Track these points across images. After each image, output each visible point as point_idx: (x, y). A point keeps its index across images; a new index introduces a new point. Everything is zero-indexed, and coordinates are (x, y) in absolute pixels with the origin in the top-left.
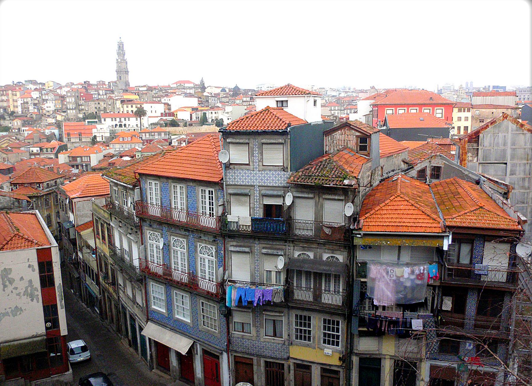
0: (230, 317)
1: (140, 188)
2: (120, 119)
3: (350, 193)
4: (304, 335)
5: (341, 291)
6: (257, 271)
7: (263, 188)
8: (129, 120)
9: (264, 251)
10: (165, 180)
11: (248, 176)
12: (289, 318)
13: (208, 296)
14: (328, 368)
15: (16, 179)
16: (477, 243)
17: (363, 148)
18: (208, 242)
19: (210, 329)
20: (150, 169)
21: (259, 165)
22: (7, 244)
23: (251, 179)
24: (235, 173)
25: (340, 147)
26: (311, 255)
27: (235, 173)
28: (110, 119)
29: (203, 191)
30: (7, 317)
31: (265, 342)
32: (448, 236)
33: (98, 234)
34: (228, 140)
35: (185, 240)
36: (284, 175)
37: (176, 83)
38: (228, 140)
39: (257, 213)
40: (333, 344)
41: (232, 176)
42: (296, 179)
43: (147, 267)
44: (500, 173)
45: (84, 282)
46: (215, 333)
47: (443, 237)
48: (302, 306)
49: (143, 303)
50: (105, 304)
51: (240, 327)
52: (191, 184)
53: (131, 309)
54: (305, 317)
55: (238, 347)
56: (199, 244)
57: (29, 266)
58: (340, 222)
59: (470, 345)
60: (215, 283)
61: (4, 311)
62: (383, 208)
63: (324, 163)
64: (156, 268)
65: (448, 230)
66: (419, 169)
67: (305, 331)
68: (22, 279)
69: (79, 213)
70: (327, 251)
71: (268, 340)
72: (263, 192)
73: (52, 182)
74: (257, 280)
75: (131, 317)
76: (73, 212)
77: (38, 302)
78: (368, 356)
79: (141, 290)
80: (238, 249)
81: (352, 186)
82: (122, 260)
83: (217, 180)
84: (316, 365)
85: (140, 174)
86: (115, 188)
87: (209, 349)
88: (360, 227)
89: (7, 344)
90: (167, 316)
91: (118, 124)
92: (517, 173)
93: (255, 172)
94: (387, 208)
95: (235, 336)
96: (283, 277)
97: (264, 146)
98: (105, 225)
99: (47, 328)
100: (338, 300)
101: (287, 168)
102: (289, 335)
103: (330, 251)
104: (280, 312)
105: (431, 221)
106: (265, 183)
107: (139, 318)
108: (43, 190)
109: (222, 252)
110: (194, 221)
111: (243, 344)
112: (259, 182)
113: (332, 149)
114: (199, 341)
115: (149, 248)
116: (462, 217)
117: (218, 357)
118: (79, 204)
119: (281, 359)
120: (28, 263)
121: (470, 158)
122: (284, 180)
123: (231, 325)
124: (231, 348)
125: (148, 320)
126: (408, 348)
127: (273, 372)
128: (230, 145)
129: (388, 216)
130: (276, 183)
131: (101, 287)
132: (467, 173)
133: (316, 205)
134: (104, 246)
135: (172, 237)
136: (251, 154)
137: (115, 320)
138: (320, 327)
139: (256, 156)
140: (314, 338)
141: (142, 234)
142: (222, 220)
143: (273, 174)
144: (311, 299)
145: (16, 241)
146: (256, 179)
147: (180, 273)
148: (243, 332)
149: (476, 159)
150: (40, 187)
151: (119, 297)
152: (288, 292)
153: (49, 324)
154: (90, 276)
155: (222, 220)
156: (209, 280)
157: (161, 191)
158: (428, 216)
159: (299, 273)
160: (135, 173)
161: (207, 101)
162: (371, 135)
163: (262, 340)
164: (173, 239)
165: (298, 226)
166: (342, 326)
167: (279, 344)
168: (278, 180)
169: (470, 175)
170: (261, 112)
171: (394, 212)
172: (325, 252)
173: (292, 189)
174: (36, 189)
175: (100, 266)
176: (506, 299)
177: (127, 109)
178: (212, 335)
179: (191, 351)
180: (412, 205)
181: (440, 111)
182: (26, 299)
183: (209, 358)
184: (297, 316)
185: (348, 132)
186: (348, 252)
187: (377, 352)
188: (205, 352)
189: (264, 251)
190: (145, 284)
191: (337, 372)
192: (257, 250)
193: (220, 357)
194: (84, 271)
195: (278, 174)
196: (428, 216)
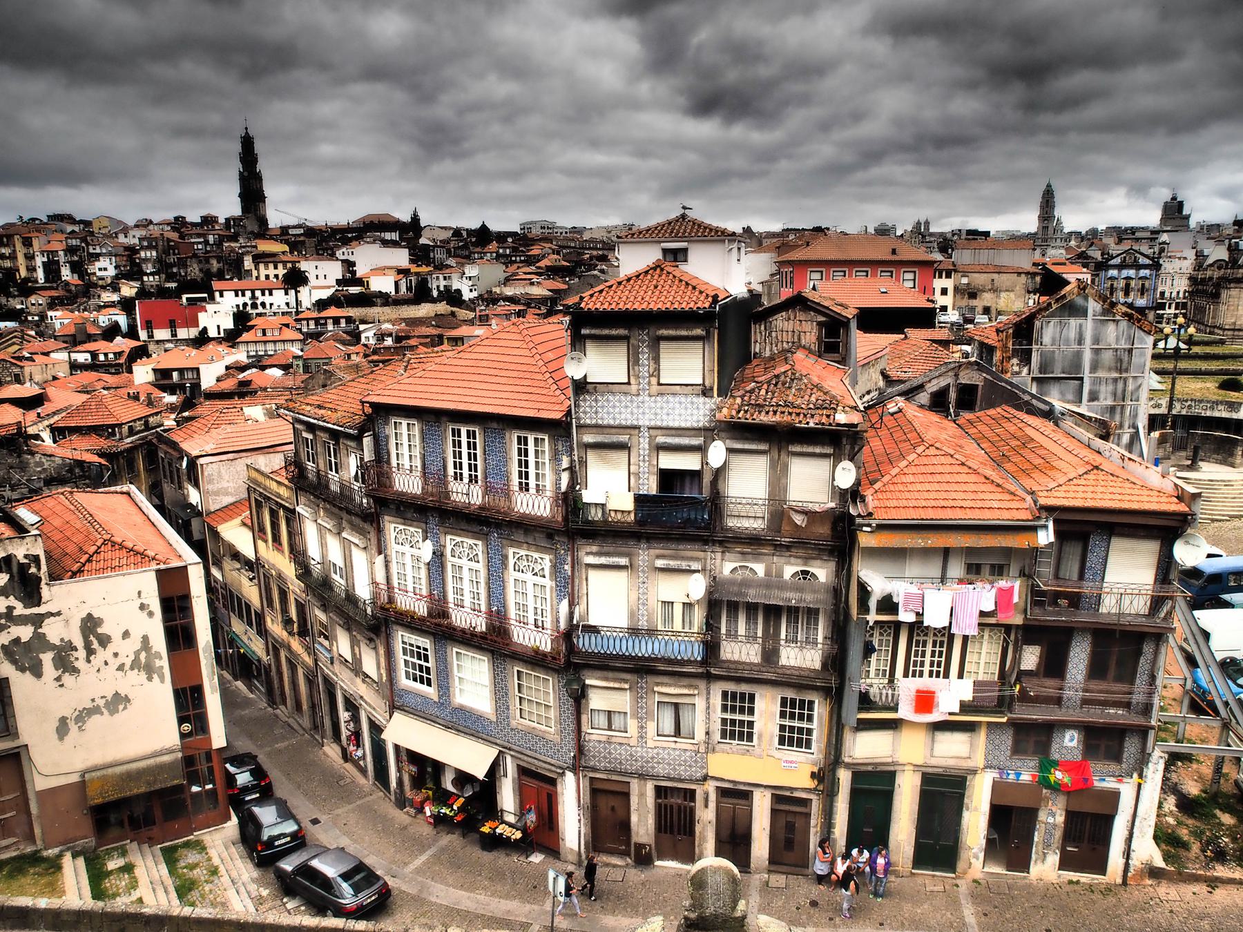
2: (253, 292)
4: (738, 731)
5: (820, 639)
6: (643, 604)
7: (659, 432)
8: (271, 294)
9: (660, 563)
10: (432, 417)
12: (708, 699)
13: (536, 660)
14: (788, 794)
15: (70, 415)
16: (1095, 542)
18: (533, 548)
19: (535, 725)
20: (396, 393)
22: (89, 561)
24: (596, 401)
26: (760, 569)
27: (596, 401)
29: (523, 441)
30: (96, 717)
32: (1046, 527)
33: (262, 530)
34: (583, 332)
35: (480, 543)
38: (583, 332)
40: (799, 745)
41: (591, 407)
42: (734, 413)
44: (1070, 397)
45: (226, 628)
47: (1034, 529)
48: (737, 673)
49: (380, 675)
50: (280, 673)
51: (602, 720)
52: (495, 425)
53: (346, 682)
54: (743, 695)
55: (599, 761)
56: (511, 551)
57: (142, 607)
58: (822, 500)
59: (1072, 740)
61: (89, 705)
62: (906, 470)
63: (782, 378)
64: (413, 602)
65: (1044, 515)
66: (935, 389)
68: (126, 634)
69: (210, 487)
70: (792, 560)
71: (665, 745)
72: (661, 439)
74: (643, 624)
76: (196, 485)
77: (162, 681)
78: (870, 768)
79: (375, 648)
80: (603, 560)
81: (856, 426)
82: (326, 583)
84: (762, 789)
85: (372, 405)
86: (305, 435)
87: (534, 765)
89: (99, 774)
91: (249, 303)
92: (1102, 396)
93: (640, 398)
94: (914, 469)
95: (593, 737)
96: (699, 616)
97: (663, 345)
98: (281, 512)
99: (183, 736)
100: (752, 653)
101: (712, 389)
102: (707, 733)
104: (690, 686)
105: (1007, 497)
107: (370, 705)
110: (502, 504)
111: (610, 753)
116: (1064, 488)
117: (553, 782)
118: (210, 468)
119: (691, 781)
120: (140, 601)
121: (1016, 369)
123: (584, 718)
124: (583, 762)
125: (393, 708)
126: (953, 750)
127: (671, 807)
129: (919, 487)
131: (270, 639)
132: (1027, 398)
133: (773, 466)
135: (449, 537)
136: (633, 361)
137: (305, 707)
140: (760, 736)
142: (570, 501)
145: (107, 553)
147: (468, 614)
148: (610, 728)
149: (1025, 370)
151: (316, 660)
152: (711, 648)
153: (187, 727)
154: (241, 617)
155: (570, 501)
156: (536, 626)
157: (423, 439)
158: (998, 485)
159: (733, 607)
160: (363, 403)
163: (650, 744)
164: (449, 541)
165: (731, 508)
166: (820, 710)
169: (1034, 402)
170: (646, 272)
171: (930, 478)
172: (789, 563)
173: (723, 434)
176: (1148, 649)
179: (494, 770)
180: (963, 464)
181: (910, 276)
182: (138, 677)
183: (533, 783)
184: (725, 694)
185: (801, 316)
186: (838, 563)
187: (890, 760)
188: (523, 771)
189: (660, 563)
191: (806, 803)
192: (643, 561)
193: (559, 780)
194: (224, 606)
196: (998, 485)
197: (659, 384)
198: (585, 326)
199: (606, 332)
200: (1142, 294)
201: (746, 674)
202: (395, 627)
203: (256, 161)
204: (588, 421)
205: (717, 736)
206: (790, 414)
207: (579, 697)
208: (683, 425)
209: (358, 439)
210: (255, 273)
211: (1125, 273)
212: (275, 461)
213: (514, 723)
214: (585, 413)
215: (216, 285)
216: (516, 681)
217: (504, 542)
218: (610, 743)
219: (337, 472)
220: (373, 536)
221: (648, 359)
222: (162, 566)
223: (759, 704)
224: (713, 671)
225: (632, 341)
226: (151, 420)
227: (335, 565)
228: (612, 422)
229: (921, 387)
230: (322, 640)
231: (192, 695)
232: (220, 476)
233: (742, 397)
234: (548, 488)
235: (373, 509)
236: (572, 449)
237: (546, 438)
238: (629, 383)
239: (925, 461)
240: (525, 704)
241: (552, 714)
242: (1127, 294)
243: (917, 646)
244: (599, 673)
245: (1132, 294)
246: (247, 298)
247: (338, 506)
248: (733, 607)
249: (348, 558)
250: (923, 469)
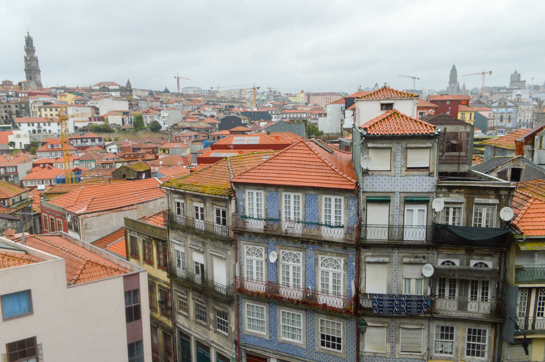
2: (39, 124)
8: (49, 125)
28: (26, 124)
37: (99, 85)
91: (37, 130)
161: (137, 105)
177: (46, 113)
200: (509, 121)
203: (34, 51)
210: (39, 113)
211: (500, 110)
215: (16, 120)
242: (501, 120)
245: (504, 121)
246: (35, 127)
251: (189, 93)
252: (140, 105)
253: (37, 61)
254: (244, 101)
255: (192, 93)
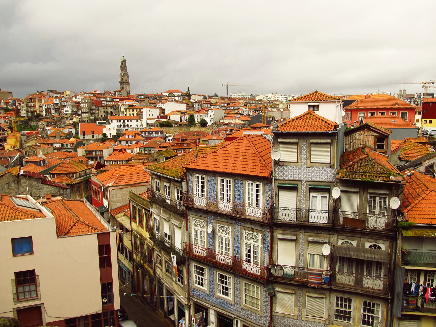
0: (274, 298)
1: (187, 181)
2: (124, 121)
3: (394, 188)
5: (382, 276)
6: (302, 256)
8: (131, 121)
11: (296, 172)
13: (252, 278)
17: (380, 147)
21: (306, 162)
23: (299, 175)
25: (359, 145)
26: (354, 243)
31: (305, 321)
33: (135, 218)
34: (279, 140)
36: (330, 171)
37: (168, 92)
38: (279, 140)
39: (303, 205)
43: (191, 250)
46: (258, 311)
52: (239, 178)
54: (346, 300)
56: (244, 231)
60: (260, 266)
66: (427, 165)
67: (345, 312)
69: (112, 199)
70: (369, 240)
71: (309, 320)
73: (83, 172)
75: (168, 291)
76: (107, 198)
81: (400, 182)
83: (267, 175)
85: (187, 169)
88: (407, 219)
90: (208, 293)
91: (122, 125)
93: (302, 168)
99: (103, 303)
101: (334, 165)
102: (329, 316)
103: (373, 240)
104: (322, 294)
106: (312, 178)
108: (76, 180)
109: (269, 239)
111: (285, 322)
112: (307, 178)
113: (351, 147)
114: (240, 317)
115: (193, 233)
122: (330, 176)
128: (281, 145)
130: (322, 178)
131: (135, 264)
134: (142, 230)
135: (217, 224)
136: (299, 153)
138: (360, 309)
139: (304, 154)
140: (354, 319)
141: (187, 221)
143: (320, 171)
144: (352, 283)
145: (78, 226)
146: (304, 175)
150: (73, 177)
153: (105, 300)
154: (123, 253)
161: (193, 106)
162: (389, 135)
163: (303, 319)
167: (319, 323)
168: (325, 176)
170: (304, 116)
172: (368, 241)
174: (71, 178)
175: (135, 245)
177: (130, 113)
178: (254, 312)
184: (337, 298)
185: (366, 133)
189: (310, 239)
190: (188, 265)
195: (325, 171)
197: (311, 163)
198: (280, 138)
199: (288, 140)
201: (348, 290)
202: (192, 262)
204: (280, 178)
205: (334, 317)
206: (369, 176)
207: (272, 297)
208: (321, 180)
209: (181, 182)
210: (125, 113)
212: (143, 189)
213: (242, 306)
214: (279, 174)
216: (244, 287)
217: (241, 227)
218: (285, 317)
219: (169, 195)
220: (184, 223)
221: (306, 152)
222: (99, 232)
223: (353, 304)
224: (333, 287)
225: (300, 144)
226: (87, 171)
227: (166, 234)
228: (290, 178)
229: (421, 164)
230: (158, 265)
231: (108, 286)
232: (116, 195)
233: (347, 168)
234: (261, 205)
235: (185, 211)
236: (272, 189)
237: (261, 184)
238: (297, 162)
239: (430, 197)
240: (248, 297)
241: (259, 302)
243: (429, 281)
244: (281, 286)
246: (122, 123)
247: (170, 209)
248: (342, 260)
249: (172, 231)
250: (429, 201)
251: (235, 97)
252: (195, 106)
253: (128, 76)
254: (277, 103)
255: (238, 97)
